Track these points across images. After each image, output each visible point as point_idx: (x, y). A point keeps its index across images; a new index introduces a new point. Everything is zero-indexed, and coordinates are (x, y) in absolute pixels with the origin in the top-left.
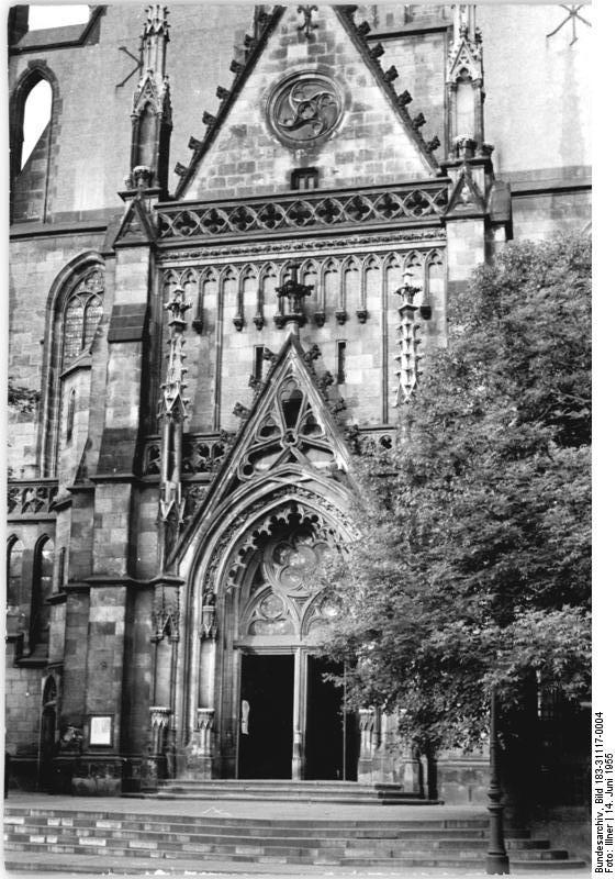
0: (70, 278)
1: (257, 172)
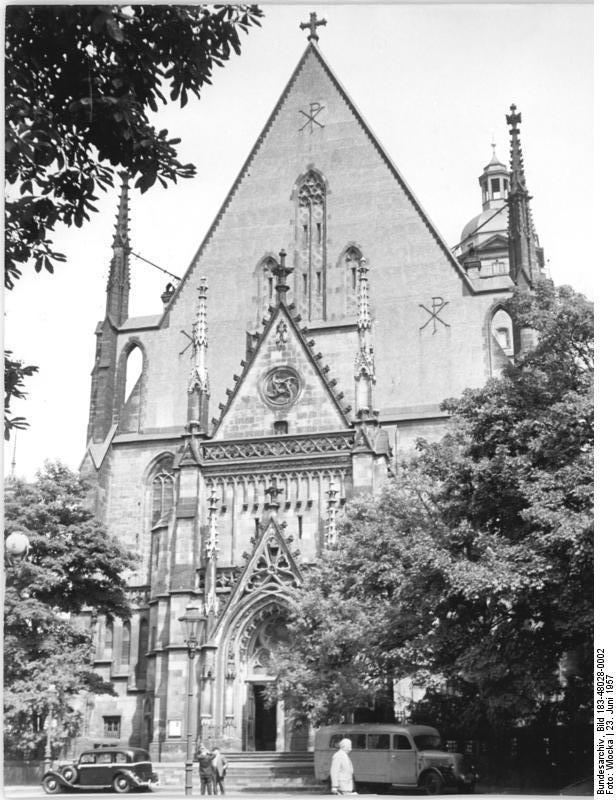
1: (255, 422)
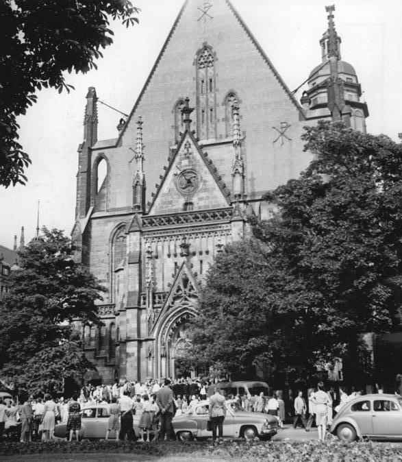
0: (116, 232)
1: (174, 204)
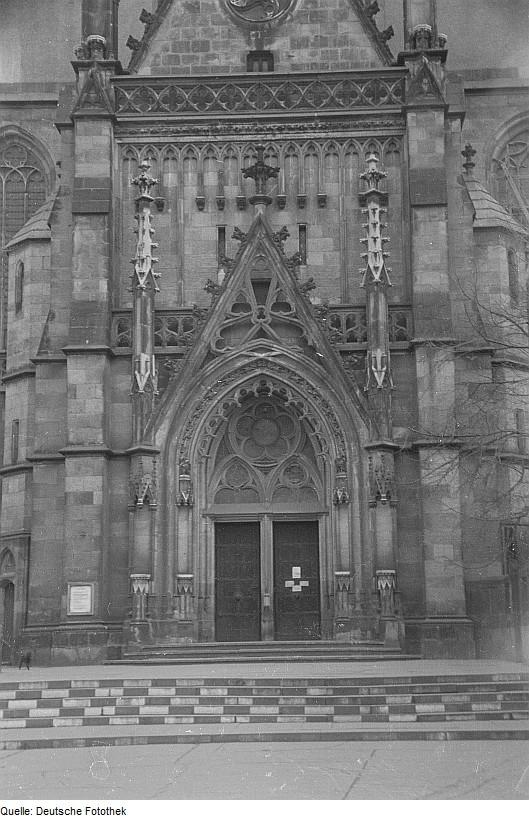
1: (211, 51)
